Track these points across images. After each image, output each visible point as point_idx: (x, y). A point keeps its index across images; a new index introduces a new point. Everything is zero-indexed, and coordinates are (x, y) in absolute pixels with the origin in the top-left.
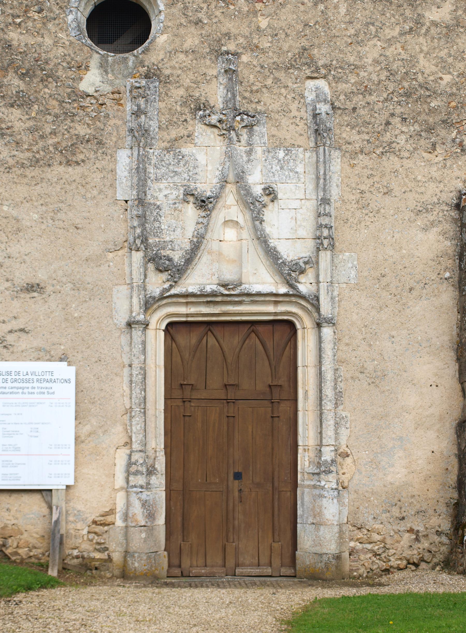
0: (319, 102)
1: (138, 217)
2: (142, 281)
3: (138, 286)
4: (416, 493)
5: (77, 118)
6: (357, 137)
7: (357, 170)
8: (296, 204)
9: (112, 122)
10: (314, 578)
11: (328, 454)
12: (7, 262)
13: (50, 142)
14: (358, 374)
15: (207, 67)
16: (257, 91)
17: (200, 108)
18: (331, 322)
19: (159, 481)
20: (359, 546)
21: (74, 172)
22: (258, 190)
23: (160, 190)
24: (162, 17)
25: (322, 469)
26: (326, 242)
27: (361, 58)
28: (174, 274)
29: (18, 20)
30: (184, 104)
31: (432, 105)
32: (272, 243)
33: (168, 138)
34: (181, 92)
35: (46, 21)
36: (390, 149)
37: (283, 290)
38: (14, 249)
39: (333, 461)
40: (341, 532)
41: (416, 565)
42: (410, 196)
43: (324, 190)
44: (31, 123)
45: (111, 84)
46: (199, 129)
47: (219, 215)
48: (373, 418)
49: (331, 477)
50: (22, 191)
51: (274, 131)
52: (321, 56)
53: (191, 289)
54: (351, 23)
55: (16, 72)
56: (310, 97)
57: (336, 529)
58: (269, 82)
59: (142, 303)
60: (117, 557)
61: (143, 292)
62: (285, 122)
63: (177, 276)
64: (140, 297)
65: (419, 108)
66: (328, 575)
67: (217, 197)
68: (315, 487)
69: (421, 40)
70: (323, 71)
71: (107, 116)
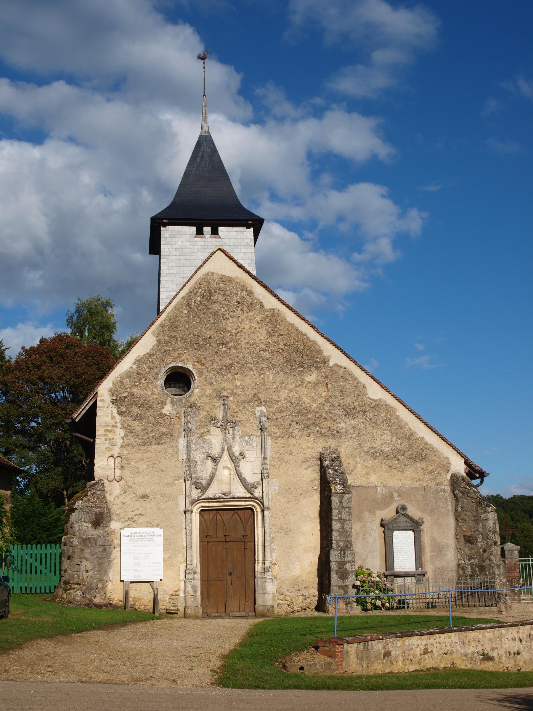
0: (262, 416)
1: (188, 466)
4: (304, 579)
5: (162, 425)
6: (278, 431)
7: (278, 444)
8: (253, 459)
9: (176, 426)
10: (263, 616)
11: (268, 564)
12: (134, 486)
13: (151, 435)
14: (280, 530)
15: (215, 402)
16: (236, 412)
17: (213, 420)
18: (268, 508)
19: (198, 576)
20: (281, 602)
21: (161, 447)
22: (237, 454)
23: (197, 454)
24: (196, 382)
25: (265, 570)
26: (266, 475)
27: (279, 397)
29: (137, 384)
30: (206, 418)
31: (309, 416)
32: (243, 476)
33: (200, 432)
34: (205, 413)
35: (148, 384)
36: (291, 436)
37: (248, 495)
38: (137, 480)
39: (270, 567)
40: (274, 596)
41: (305, 610)
42: (300, 455)
43: (265, 454)
44: (143, 427)
45: (176, 410)
46: (213, 429)
47: (221, 464)
48: (286, 548)
49: (269, 573)
50: (139, 456)
51: (243, 429)
52: (263, 397)
53: (210, 496)
54: (274, 383)
55: (136, 406)
56: (258, 414)
57: (272, 595)
58: (241, 408)
60: (181, 609)
62: (248, 425)
65: (303, 418)
66: (269, 614)
67: (220, 457)
68: (263, 578)
69: (304, 389)
70: (264, 403)
71: (174, 424)
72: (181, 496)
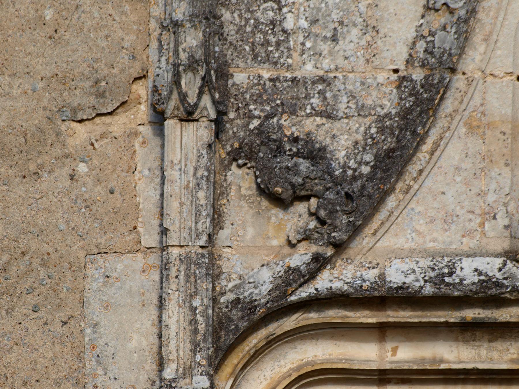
2: (204, 240)
3: (187, 260)
28: (332, 213)
59: (202, 327)
61: (205, 285)
63: (344, 219)
64: (196, 303)
72: (120, 264)
